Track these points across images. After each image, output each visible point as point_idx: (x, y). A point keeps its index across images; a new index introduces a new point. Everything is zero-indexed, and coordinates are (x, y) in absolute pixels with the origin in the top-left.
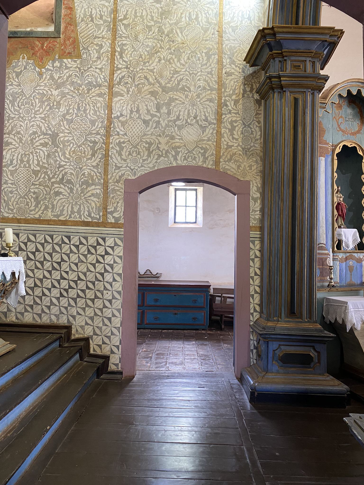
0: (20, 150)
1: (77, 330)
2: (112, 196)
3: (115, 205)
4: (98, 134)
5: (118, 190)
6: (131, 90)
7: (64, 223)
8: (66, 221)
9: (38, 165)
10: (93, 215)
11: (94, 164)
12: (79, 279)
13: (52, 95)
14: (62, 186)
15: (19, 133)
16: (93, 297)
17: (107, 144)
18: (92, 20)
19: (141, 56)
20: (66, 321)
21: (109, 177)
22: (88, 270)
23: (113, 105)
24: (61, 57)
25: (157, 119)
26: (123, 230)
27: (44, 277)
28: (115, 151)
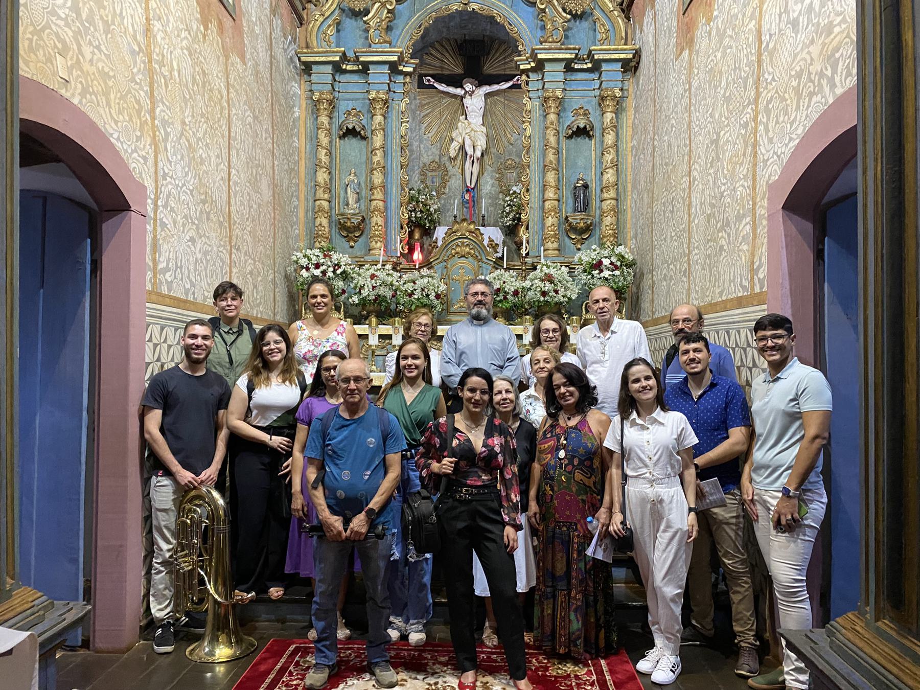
0: (700, 186)
11: (744, 173)
26: (765, 307)
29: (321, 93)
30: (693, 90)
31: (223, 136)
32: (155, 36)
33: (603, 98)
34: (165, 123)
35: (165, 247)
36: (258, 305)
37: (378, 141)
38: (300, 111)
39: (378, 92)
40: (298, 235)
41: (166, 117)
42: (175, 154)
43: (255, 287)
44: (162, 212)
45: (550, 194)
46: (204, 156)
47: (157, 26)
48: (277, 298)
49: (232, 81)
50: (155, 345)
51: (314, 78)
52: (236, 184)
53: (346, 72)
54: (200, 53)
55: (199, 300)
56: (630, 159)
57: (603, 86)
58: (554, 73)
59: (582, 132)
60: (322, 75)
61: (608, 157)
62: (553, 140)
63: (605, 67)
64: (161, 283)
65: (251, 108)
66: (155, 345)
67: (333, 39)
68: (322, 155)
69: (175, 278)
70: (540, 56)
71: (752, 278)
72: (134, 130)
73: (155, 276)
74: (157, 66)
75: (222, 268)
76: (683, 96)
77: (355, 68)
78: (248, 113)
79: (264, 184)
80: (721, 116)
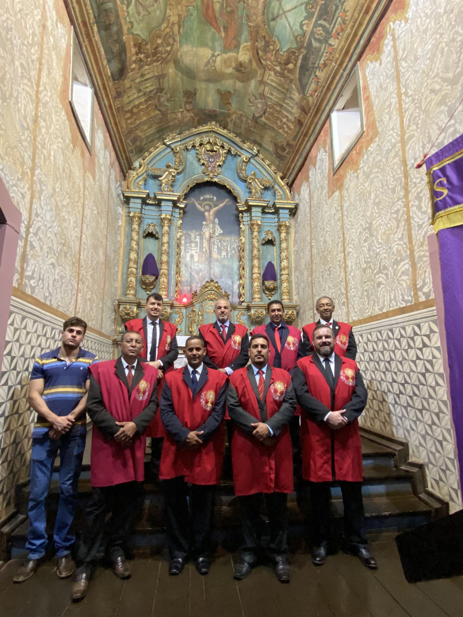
1: (413, 451)
2: (419, 265)
3: (423, 277)
4: (398, 201)
5: (424, 256)
6: (420, 122)
7: (386, 315)
8: (388, 312)
9: (365, 262)
10: (406, 298)
11: (400, 236)
12: (406, 382)
13: (365, 189)
14: (381, 275)
15: (353, 240)
16: (420, 407)
17: (407, 205)
18: (382, 89)
19: (424, 72)
20: (403, 437)
21: (414, 243)
22: (412, 371)
23: (407, 155)
24: (367, 149)
25: (452, 129)
26: (434, 308)
27: (382, 380)
28: (415, 208)
29: (135, 213)
30: (345, 208)
31: (79, 213)
32: (40, 128)
33: (280, 226)
34: (41, 182)
35: (32, 261)
36: (93, 320)
37: (165, 239)
38: (122, 222)
39: (166, 215)
40: (117, 287)
41: (42, 180)
42: (46, 204)
43: (91, 308)
44: (32, 237)
45: (256, 270)
46: (66, 217)
47: (42, 124)
48: (104, 319)
49: (87, 184)
50: (16, 330)
51: (131, 205)
52: (84, 243)
53: (148, 204)
54: (69, 158)
55: (55, 306)
56: (293, 256)
57: (281, 220)
58: (256, 212)
59: (270, 242)
60: (136, 204)
61: (284, 254)
62: (256, 244)
63: (281, 211)
64: (26, 285)
65: (96, 206)
66: (16, 330)
67: (142, 187)
68: (134, 244)
69: (38, 285)
70: (250, 203)
71: (416, 294)
72: (17, 172)
73: (22, 279)
74: (40, 146)
75: (72, 290)
76: (335, 214)
77: (154, 203)
78: (95, 208)
79: (101, 252)
80: (372, 213)
